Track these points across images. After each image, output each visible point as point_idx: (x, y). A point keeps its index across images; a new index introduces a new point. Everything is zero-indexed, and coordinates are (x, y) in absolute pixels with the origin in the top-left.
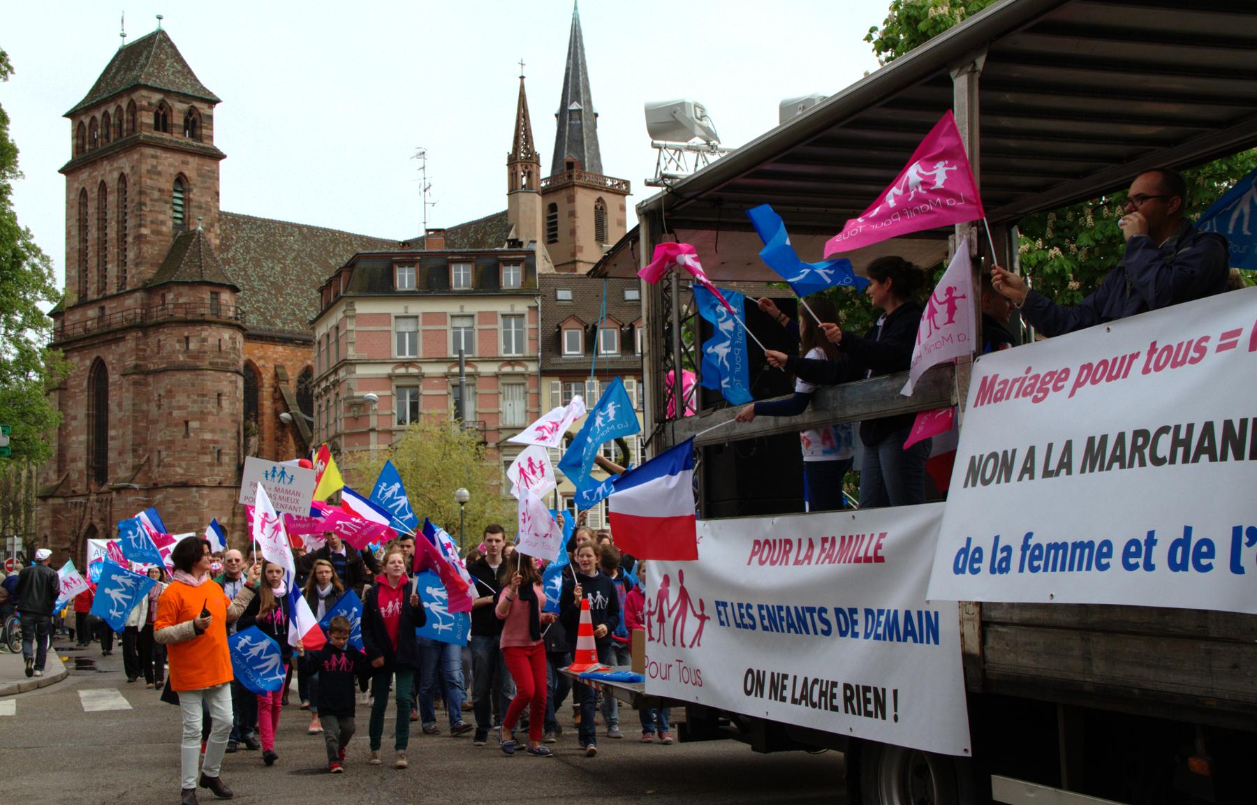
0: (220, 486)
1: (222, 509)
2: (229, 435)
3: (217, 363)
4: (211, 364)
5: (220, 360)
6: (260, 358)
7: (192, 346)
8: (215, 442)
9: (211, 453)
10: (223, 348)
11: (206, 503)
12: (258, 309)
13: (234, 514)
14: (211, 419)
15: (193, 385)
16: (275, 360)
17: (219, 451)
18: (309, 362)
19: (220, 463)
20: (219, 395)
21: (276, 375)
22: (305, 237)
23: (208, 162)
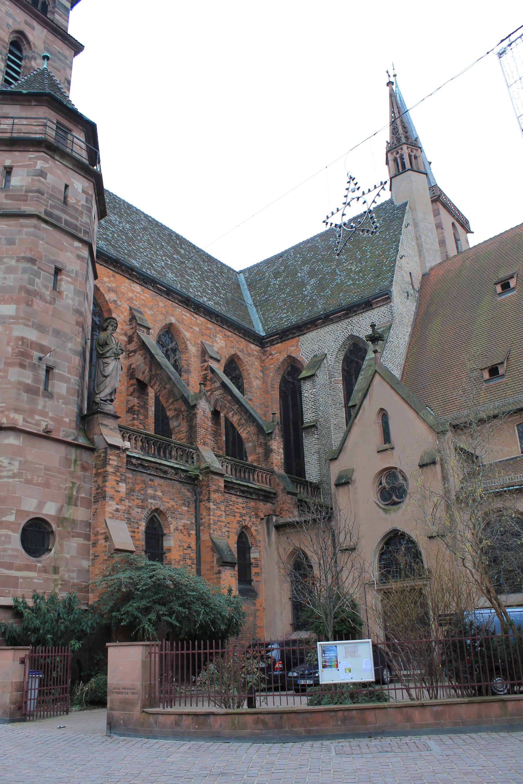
0: (46, 436)
1: (47, 485)
2: (70, 345)
3: (59, 219)
4: (46, 213)
5: (64, 217)
6: (110, 290)
7: (16, 181)
8: (42, 349)
9: (34, 367)
10: (71, 200)
11: (15, 467)
12: (106, 239)
13: (71, 500)
14: (38, 304)
15: (11, 242)
16: (130, 299)
17: (49, 370)
18: (173, 320)
19: (48, 394)
20: (58, 271)
21: (133, 318)
22: (150, 221)
23: (60, 43)
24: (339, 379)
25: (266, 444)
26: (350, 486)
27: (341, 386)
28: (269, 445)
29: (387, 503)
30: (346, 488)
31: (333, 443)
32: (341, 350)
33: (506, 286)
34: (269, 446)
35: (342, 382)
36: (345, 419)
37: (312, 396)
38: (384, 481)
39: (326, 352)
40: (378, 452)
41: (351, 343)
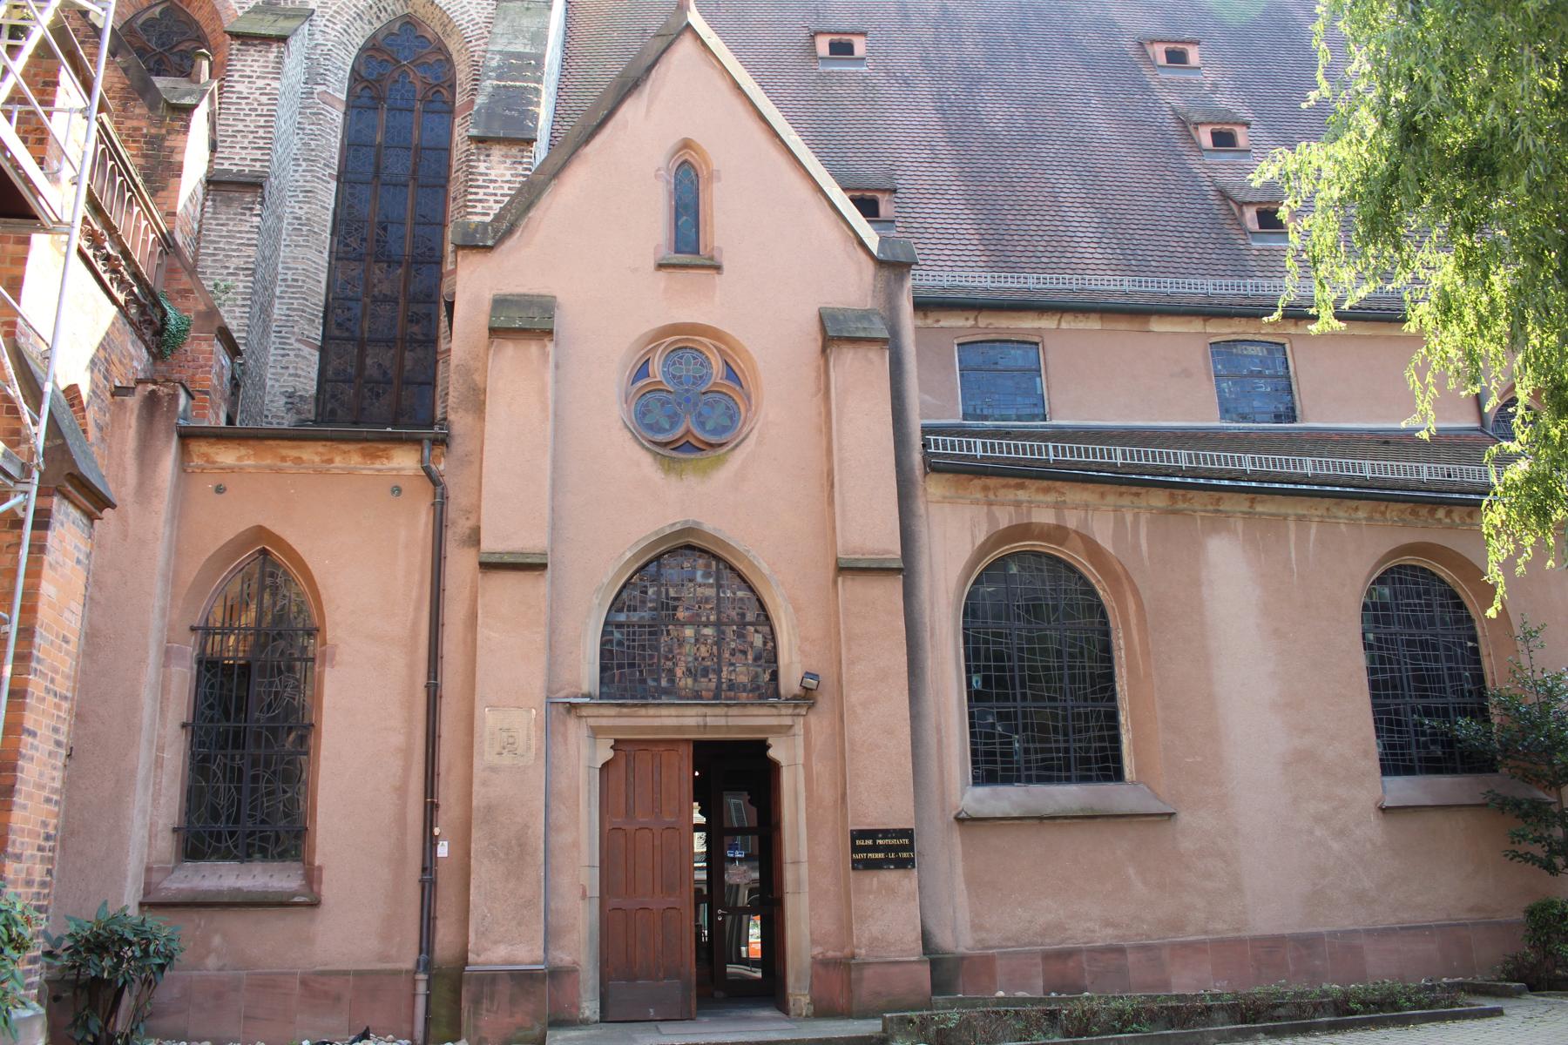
24: (338, 95)
25: (155, 142)
26: (550, 347)
27: (337, 115)
28: (172, 150)
29: (660, 438)
30: (533, 348)
31: (280, 269)
32: (366, 18)
33: (842, 49)
34: (172, 150)
35: (343, 109)
36: (330, 213)
37: (264, 99)
38: (656, 368)
39: (312, 6)
40: (661, 266)
41: (400, 12)
